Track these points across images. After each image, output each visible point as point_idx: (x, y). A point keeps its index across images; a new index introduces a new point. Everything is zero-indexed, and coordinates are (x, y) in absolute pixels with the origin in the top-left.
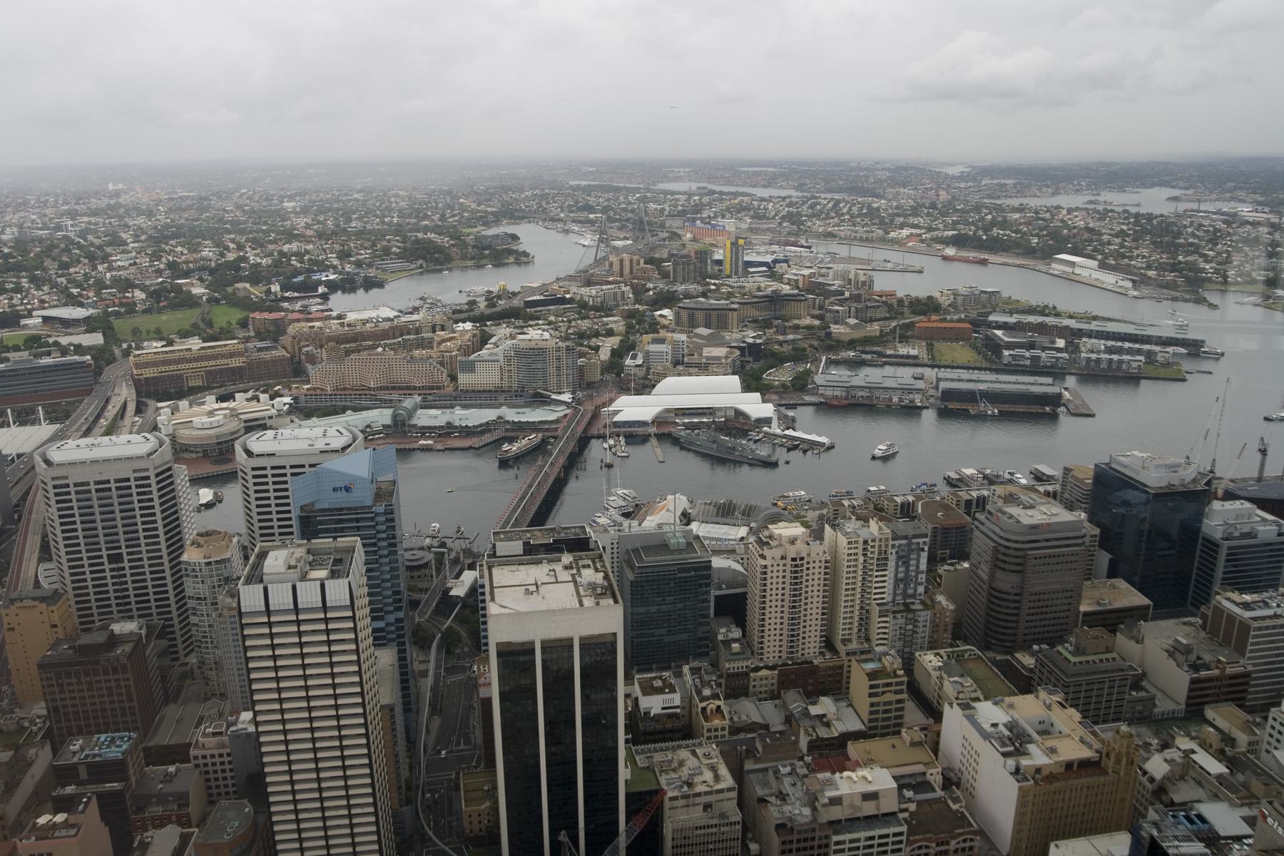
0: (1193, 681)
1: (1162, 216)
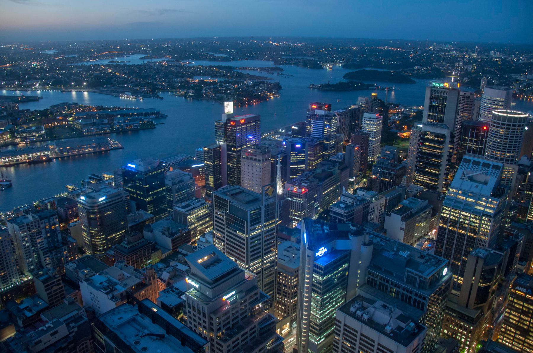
0: (172, 240)
1: (138, 65)
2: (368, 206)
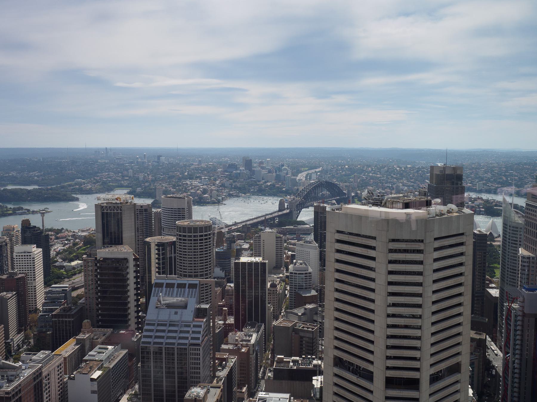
2: (41, 374)
